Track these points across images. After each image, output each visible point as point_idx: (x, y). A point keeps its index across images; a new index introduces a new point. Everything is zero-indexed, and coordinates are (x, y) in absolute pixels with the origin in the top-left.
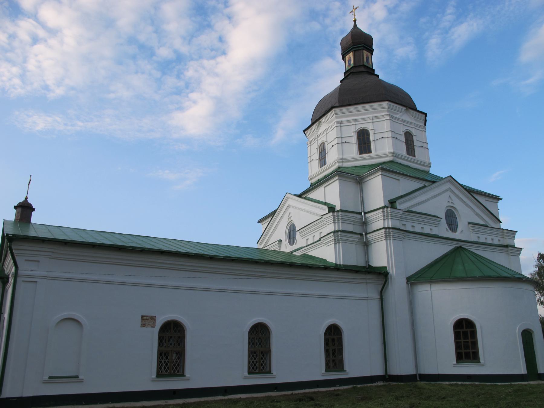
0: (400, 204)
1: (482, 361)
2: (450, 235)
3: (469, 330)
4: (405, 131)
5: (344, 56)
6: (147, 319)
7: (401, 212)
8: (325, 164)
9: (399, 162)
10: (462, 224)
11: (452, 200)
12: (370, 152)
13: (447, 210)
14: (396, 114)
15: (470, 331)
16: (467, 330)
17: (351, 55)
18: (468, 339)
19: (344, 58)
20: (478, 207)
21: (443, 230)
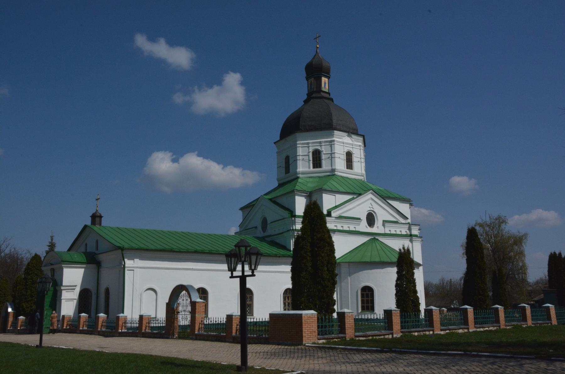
0: (333, 213)
2: (369, 230)
3: (369, 293)
7: (334, 218)
8: (289, 172)
9: (340, 175)
13: (368, 214)
14: (342, 138)
16: (368, 293)
17: (312, 79)
18: (369, 298)
21: (363, 227)
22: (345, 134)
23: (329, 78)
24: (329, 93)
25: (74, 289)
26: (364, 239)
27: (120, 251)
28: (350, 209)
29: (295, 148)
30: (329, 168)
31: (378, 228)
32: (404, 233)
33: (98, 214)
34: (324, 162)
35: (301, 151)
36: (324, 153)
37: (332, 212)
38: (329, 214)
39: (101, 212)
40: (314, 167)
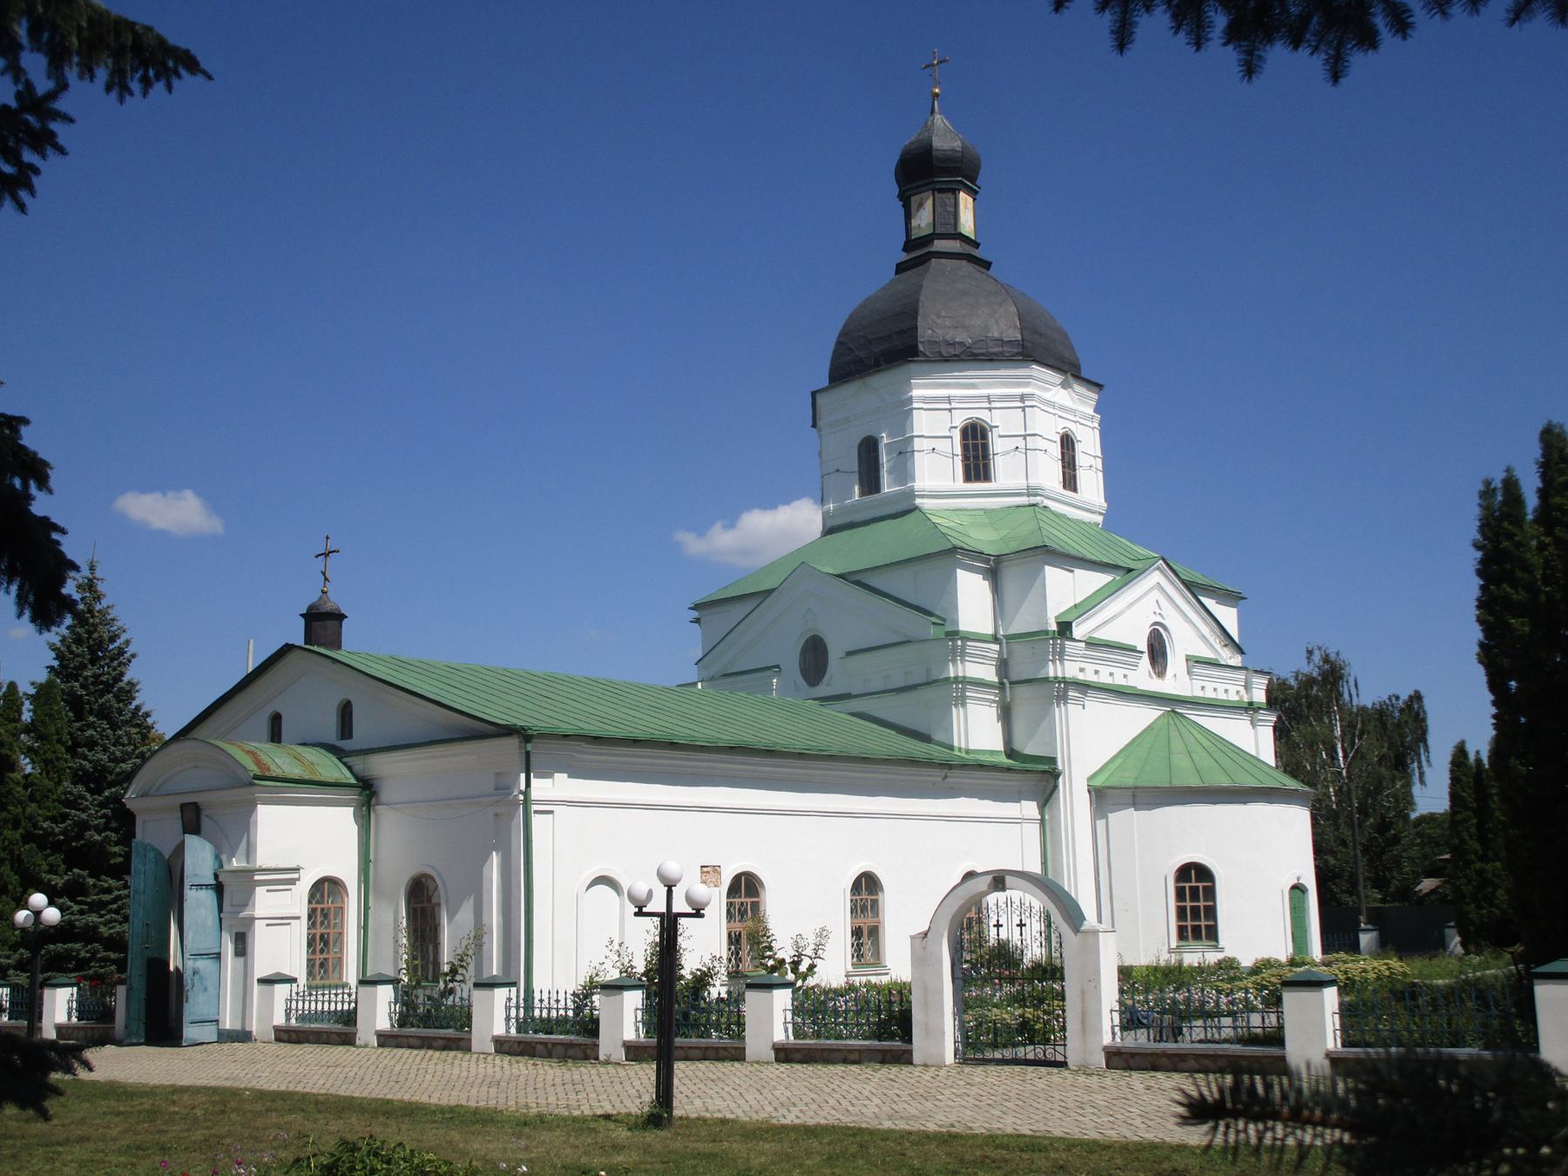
1: (1222, 943)
3: (1200, 885)
4: (1061, 432)
5: (907, 194)
6: (708, 872)
10: (1176, 662)
11: (1160, 608)
12: (986, 477)
13: (1151, 633)
14: (1048, 390)
15: (1204, 887)
19: (905, 199)
20: (1207, 624)
22: (1055, 377)
23: (973, 193)
24: (976, 244)
25: (293, 882)
26: (1146, 715)
27: (513, 743)
28: (1113, 618)
29: (902, 412)
30: (1019, 483)
31: (1177, 681)
32: (1233, 697)
33: (328, 607)
35: (925, 423)
36: (1002, 434)
37: (1074, 624)
38: (1065, 628)
39: (338, 599)
40: (968, 478)
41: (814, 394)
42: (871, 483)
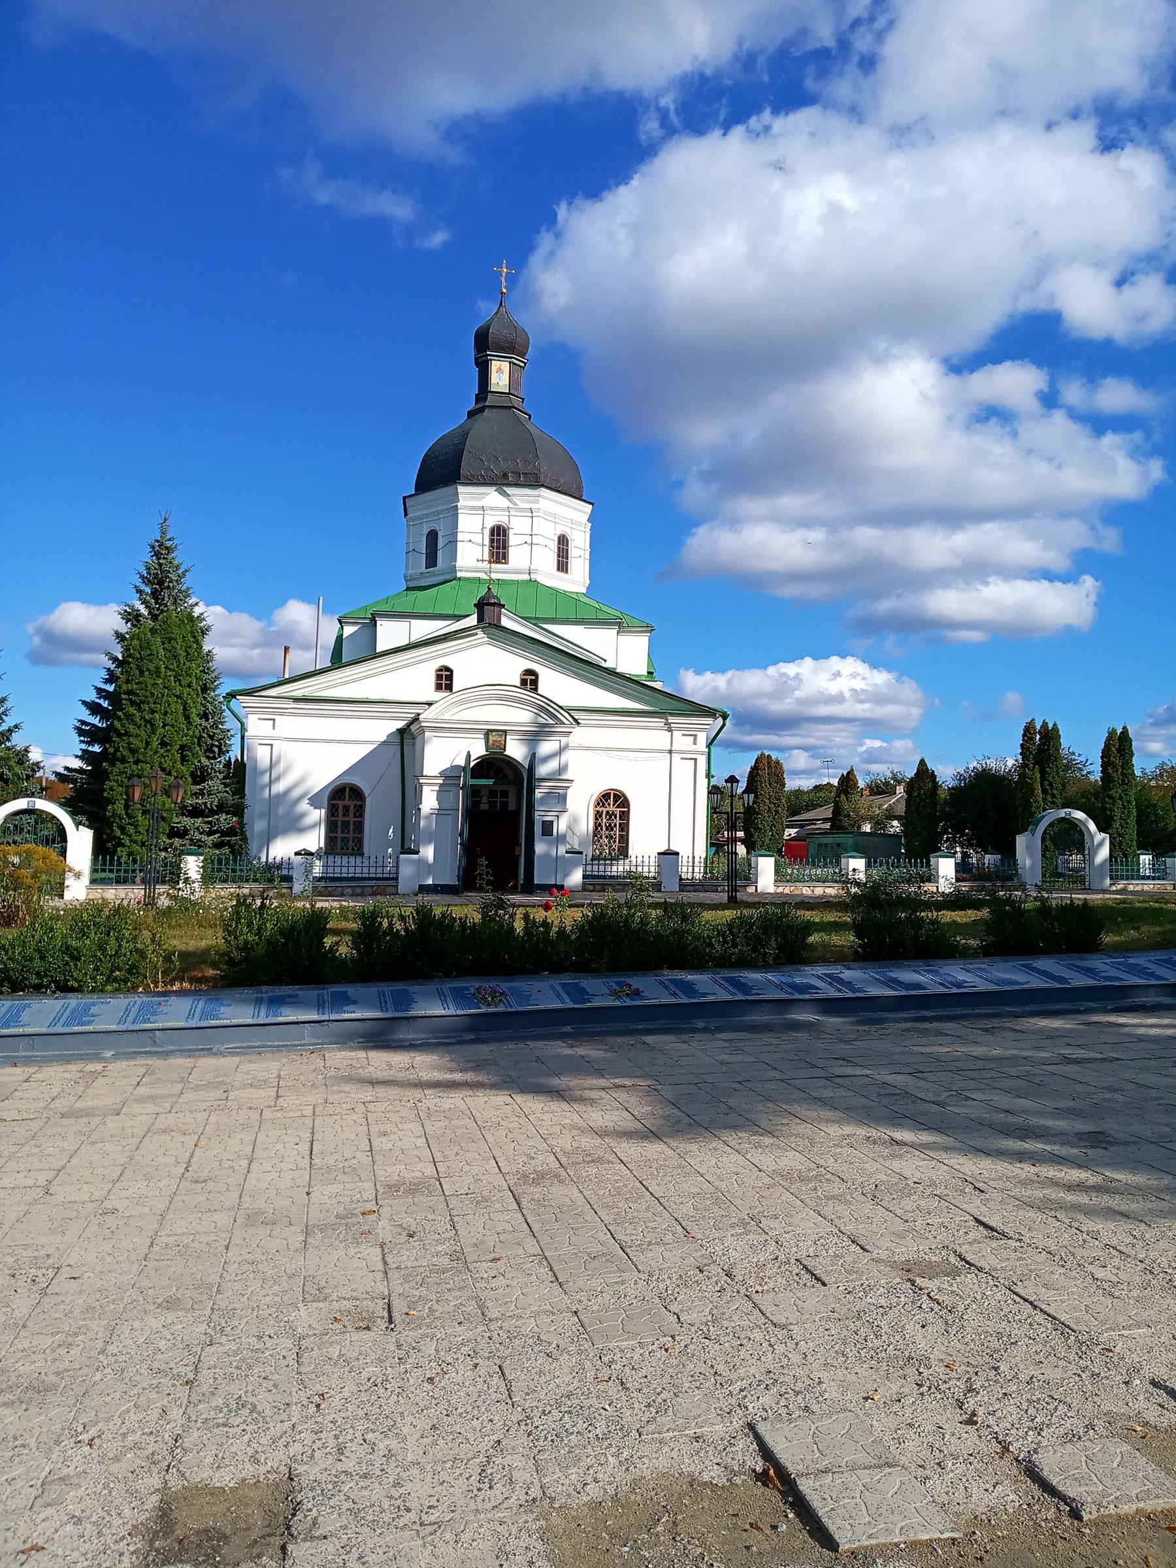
29: (453, 513)
30: (525, 565)
34: (513, 552)
41: (404, 498)
42: (432, 561)
